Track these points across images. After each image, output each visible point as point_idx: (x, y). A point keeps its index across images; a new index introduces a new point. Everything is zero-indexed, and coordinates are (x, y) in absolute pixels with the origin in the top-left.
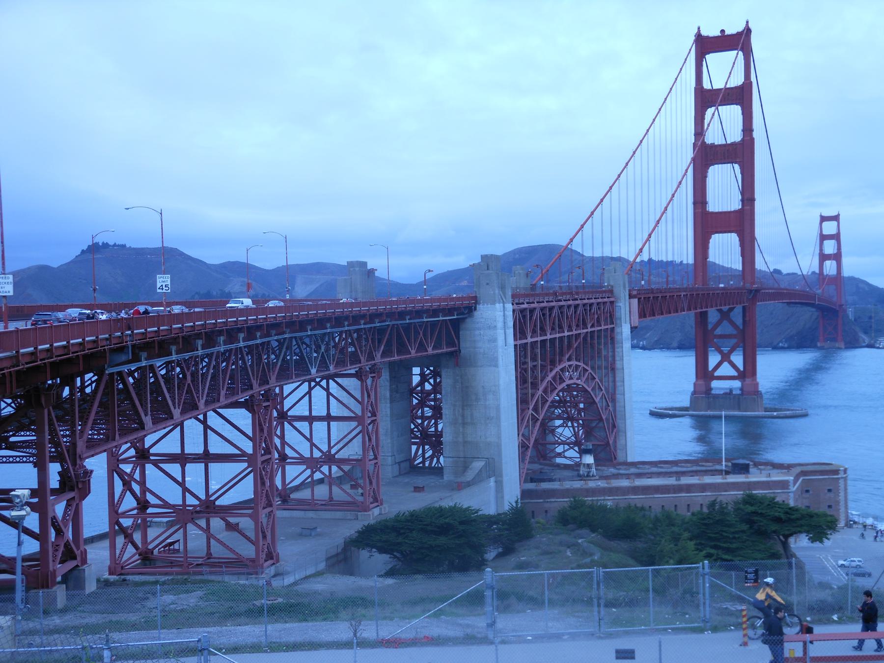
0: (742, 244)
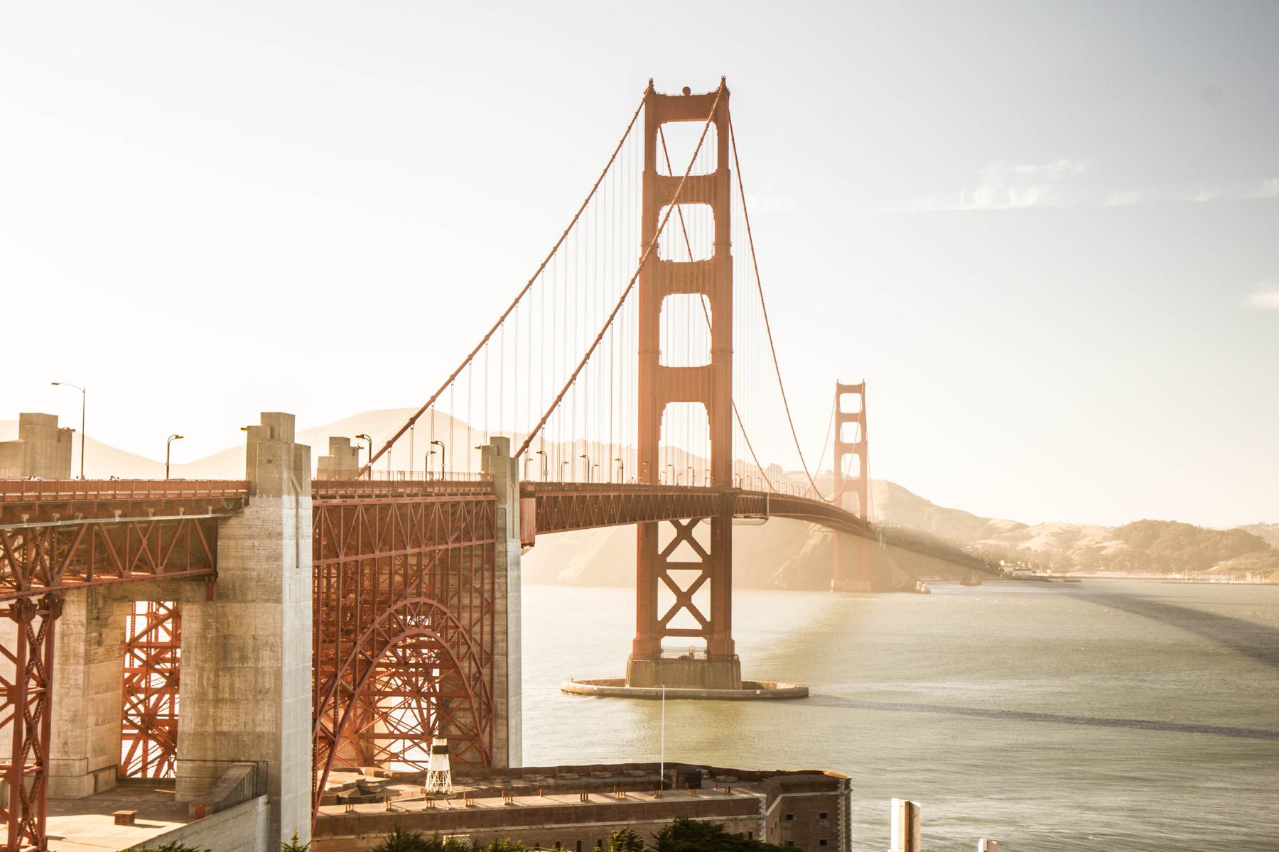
0: (712, 422)
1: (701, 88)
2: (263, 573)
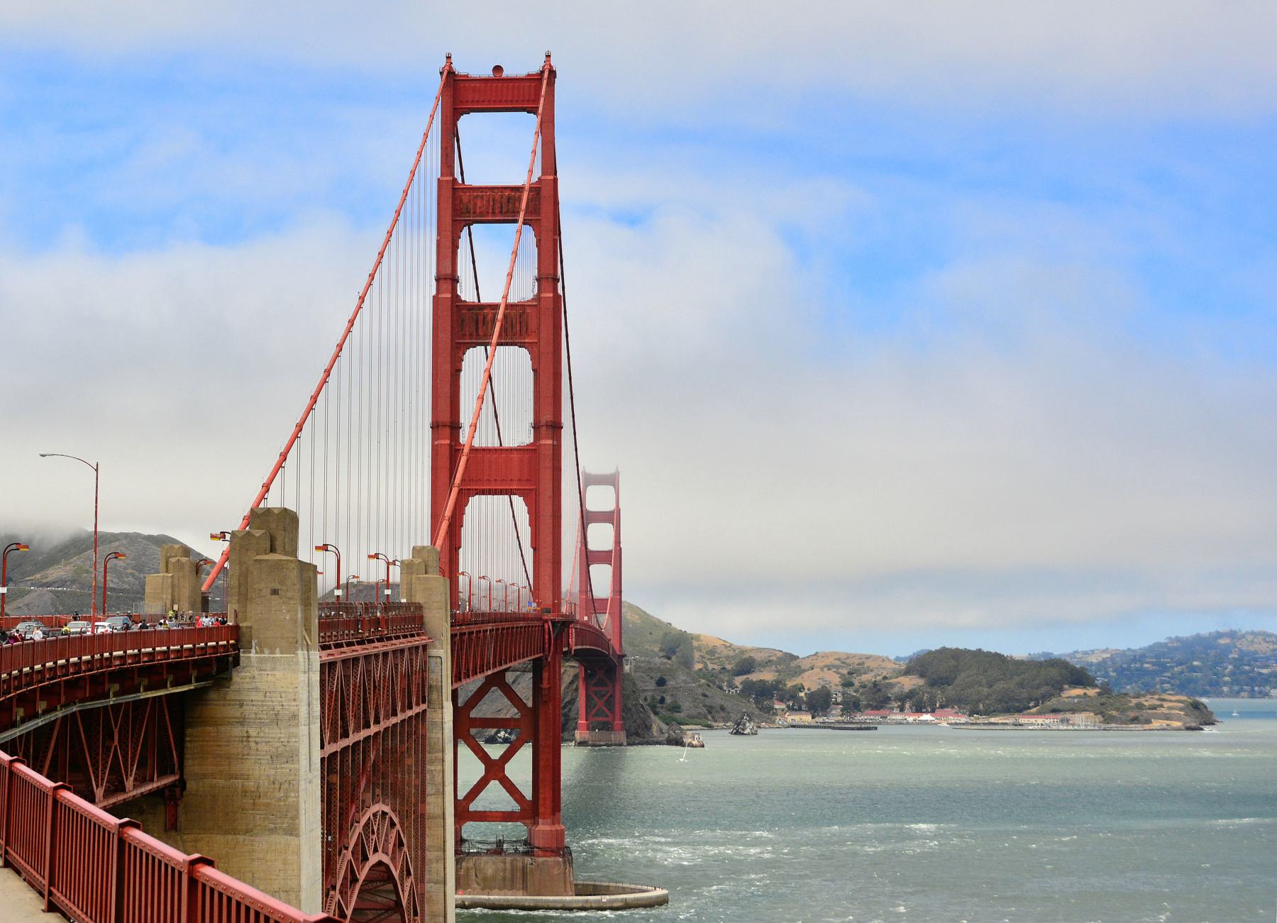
1: (516, 68)
2: (264, 784)
